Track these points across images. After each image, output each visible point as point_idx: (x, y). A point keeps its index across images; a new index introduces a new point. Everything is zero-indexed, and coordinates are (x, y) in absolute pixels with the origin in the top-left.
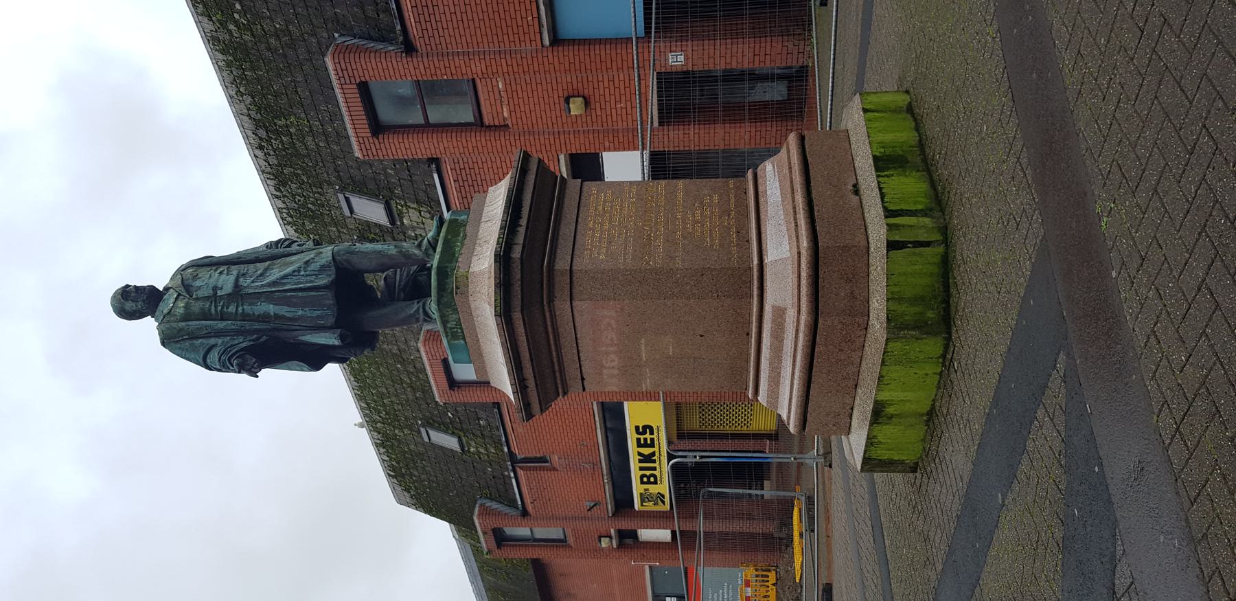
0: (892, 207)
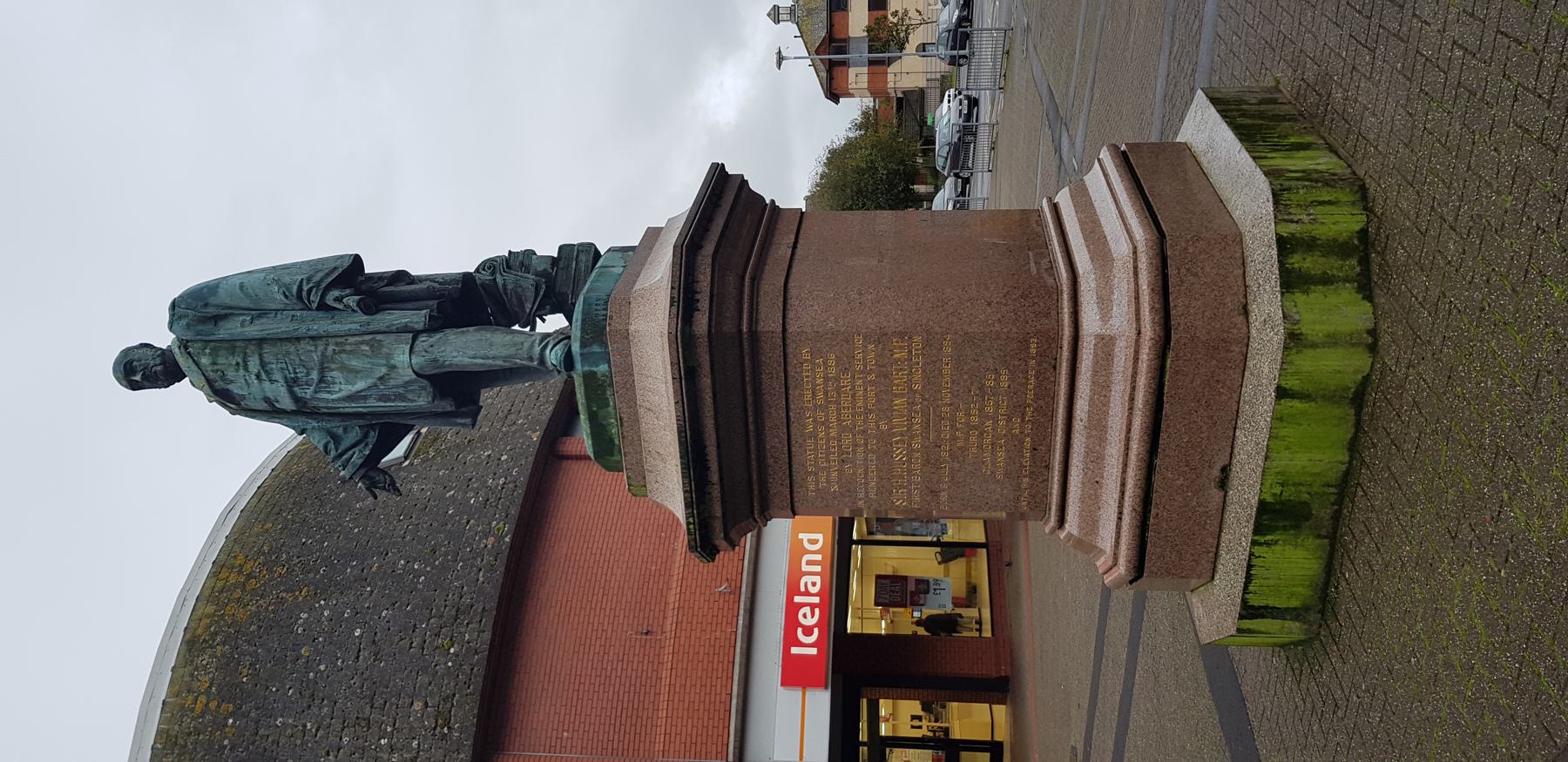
0: (1255, 601)
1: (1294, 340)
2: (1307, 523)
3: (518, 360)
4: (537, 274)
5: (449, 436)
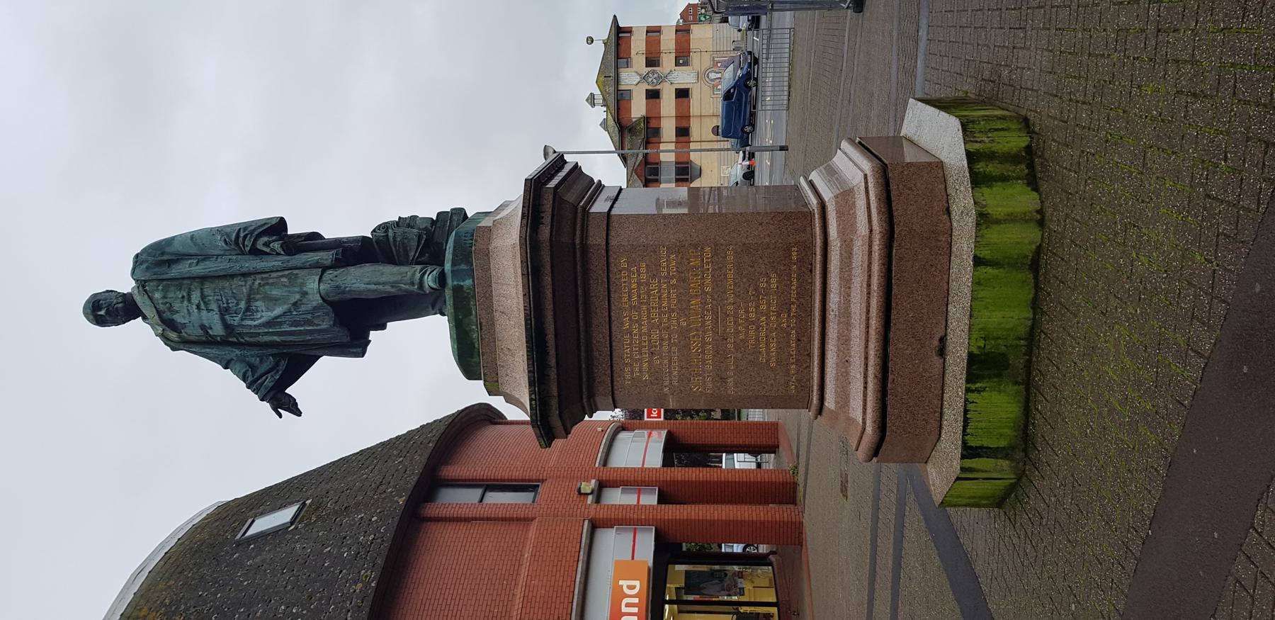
0: (973, 442)
1: (984, 219)
2: (1006, 372)
3: (403, 285)
4: (419, 229)
5: (329, 504)
